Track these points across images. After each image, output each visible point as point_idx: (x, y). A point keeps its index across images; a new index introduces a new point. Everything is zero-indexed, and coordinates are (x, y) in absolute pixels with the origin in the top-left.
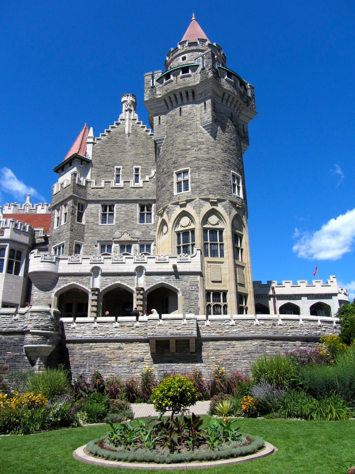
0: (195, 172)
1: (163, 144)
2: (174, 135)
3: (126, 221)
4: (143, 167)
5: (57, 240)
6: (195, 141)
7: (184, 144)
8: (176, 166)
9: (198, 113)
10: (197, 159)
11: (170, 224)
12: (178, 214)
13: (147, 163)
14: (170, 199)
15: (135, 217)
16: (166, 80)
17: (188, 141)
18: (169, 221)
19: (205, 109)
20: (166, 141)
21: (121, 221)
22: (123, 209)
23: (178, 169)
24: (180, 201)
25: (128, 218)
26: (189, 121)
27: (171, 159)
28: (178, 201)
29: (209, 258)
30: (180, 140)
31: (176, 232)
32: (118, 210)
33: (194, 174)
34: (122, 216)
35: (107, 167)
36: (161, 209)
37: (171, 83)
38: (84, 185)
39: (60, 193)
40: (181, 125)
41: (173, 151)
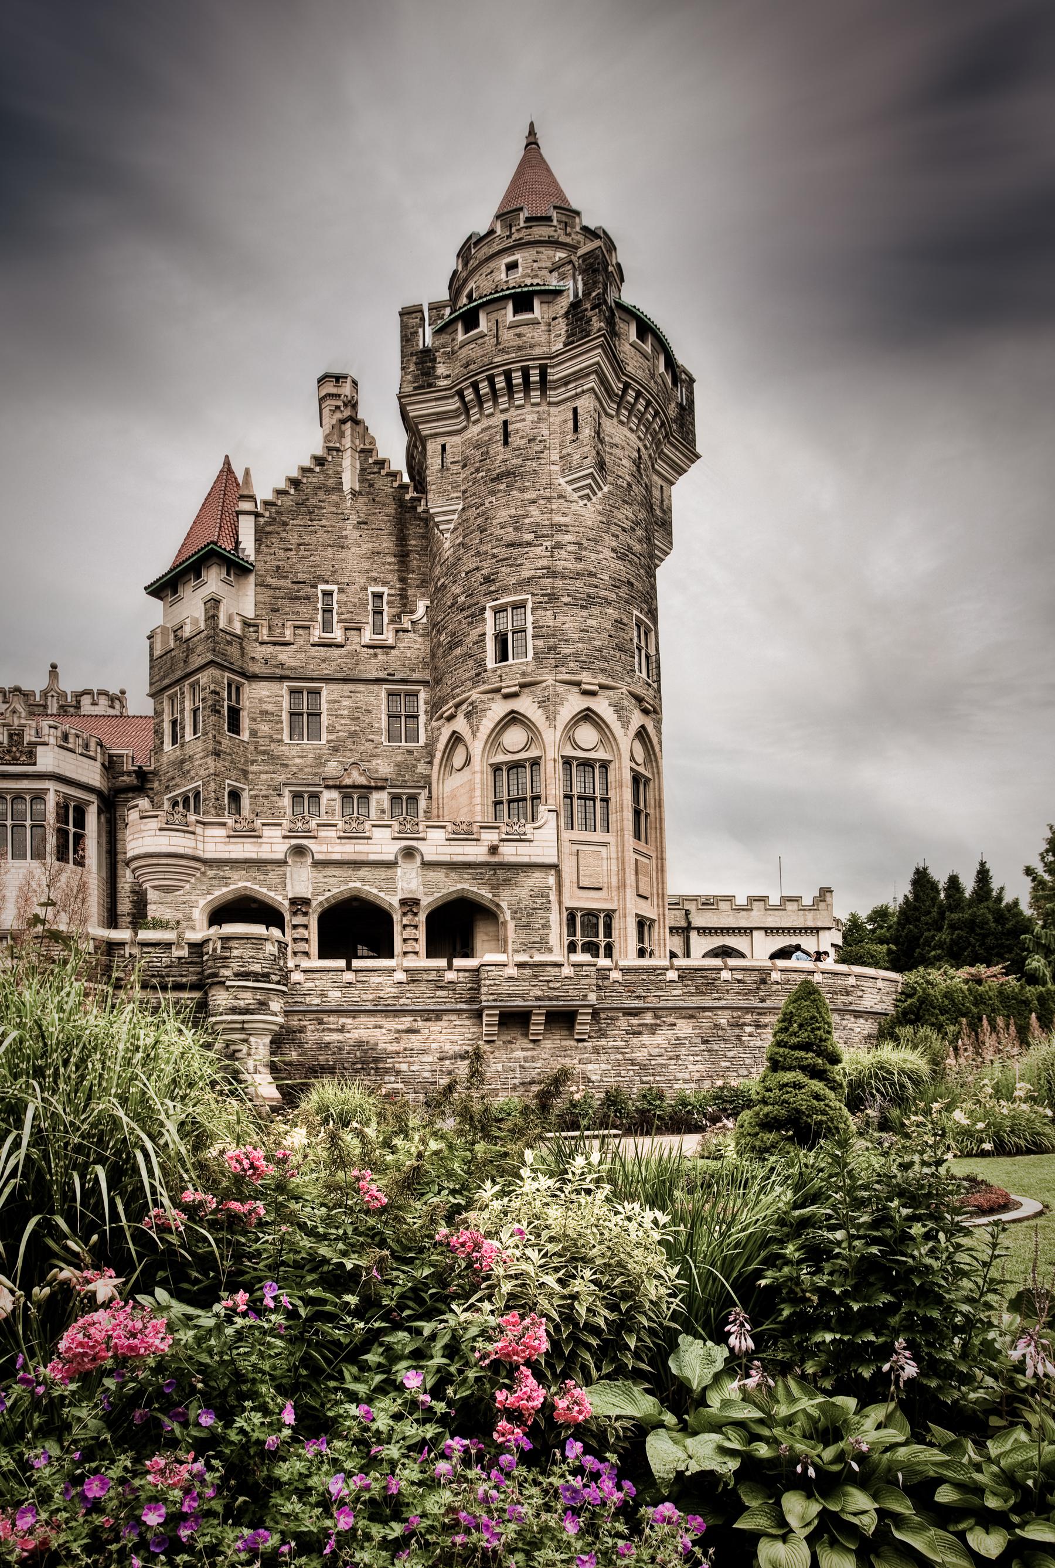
0: (545, 609)
2: (487, 502)
3: (354, 735)
5: (177, 780)
6: (548, 523)
7: (516, 529)
8: (493, 588)
9: (555, 441)
10: (552, 573)
11: (477, 747)
12: (498, 719)
14: (477, 678)
15: (377, 725)
16: (467, 331)
17: (527, 521)
18: (474, 734)
19: (576, 429)
20: (464, 518)
21: (341, 734)
22: (345, 703)
23: (497, 599)
24: (503, 685)
25: (357, 728)
26: (529, 463)
27: (477, 569)
28: (497, 685)
29: (577, 834)
30: (503, 515)
31: (491, 765)
32: (331, 706)
33: (543, 613)
34: (343, 722)
36: (450, 704)
37: (480, 341)
38: (238, 632)
40: (508, 474)
41: (483, 548)
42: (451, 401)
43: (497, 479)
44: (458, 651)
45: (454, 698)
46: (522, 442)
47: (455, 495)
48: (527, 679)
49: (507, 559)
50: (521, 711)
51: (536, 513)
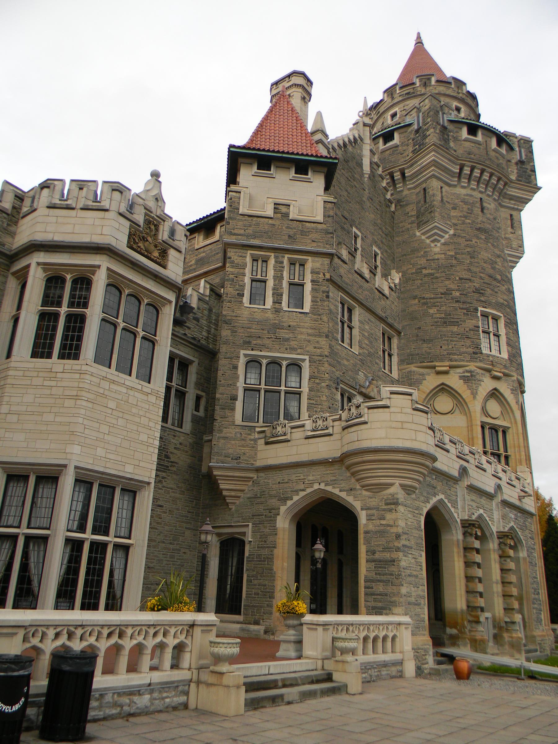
1: (443, 241)
4: (383, 257)
8: (482, 299)
13: (386, 251)
22: (367, 327)
23: (485, 308)
30: (484, 255)
35: (344, 220)
36: (447, 363)
39: (270, 221)
41: (472, 268)
43: (479, 229)
44: (455, 329)
45: (451, 360)
46: (491, 217)
47: (449, 223)
49: (489, 284)
50: (502, 391)
51: (500, 264)
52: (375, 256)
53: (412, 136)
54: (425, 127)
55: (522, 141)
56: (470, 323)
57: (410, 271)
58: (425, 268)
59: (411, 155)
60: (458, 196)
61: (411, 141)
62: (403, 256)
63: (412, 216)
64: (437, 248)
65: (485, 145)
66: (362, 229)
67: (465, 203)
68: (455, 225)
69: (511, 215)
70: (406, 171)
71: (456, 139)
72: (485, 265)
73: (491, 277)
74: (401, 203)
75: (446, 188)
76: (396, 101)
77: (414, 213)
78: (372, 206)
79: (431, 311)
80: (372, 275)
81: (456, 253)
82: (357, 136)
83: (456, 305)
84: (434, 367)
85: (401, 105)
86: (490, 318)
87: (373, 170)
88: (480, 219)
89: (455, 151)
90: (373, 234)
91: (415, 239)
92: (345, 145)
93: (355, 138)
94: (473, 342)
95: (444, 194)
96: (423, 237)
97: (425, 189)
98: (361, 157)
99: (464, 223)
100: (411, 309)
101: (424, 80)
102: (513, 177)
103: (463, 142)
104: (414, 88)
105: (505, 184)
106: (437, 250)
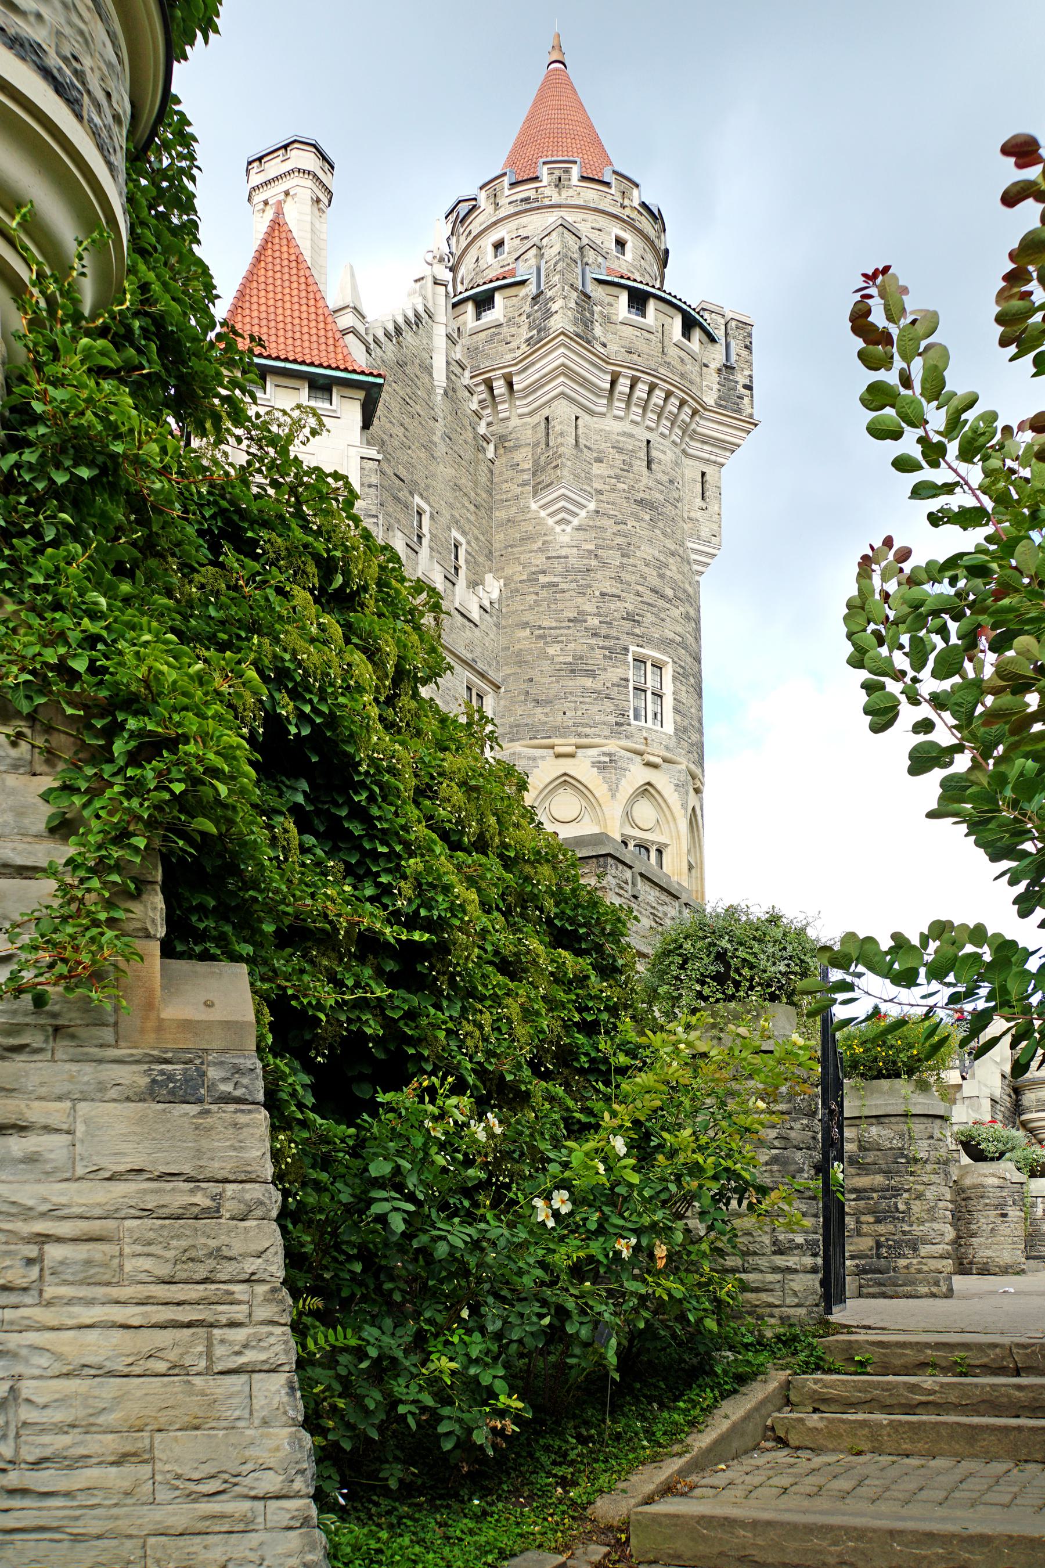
1: (576, 522)
8: (637, 631)
13: (477, 539)
35: (397, 481)
41: (626, 577)
42: (601, 375)
43: (640, 502)
44: (588, 682)
46: (665, 478)
47: (589, 489)
48: (669, 755)
51: (674, 568)
52: (456, 547)
53: (527, 308)
54: (549, 294)
55: (733, 323)
56: (613, 674)
57: (517, 578)
58: (544, 572)
59: (524, 347)
60: (606, 435)
61: (524, 317)
62: (506, 547)
63: (524, 471)
64: (564, 536)
65: (660, 335)
66: (431, 498)
67: (620, 450)
68: (600, 492)
69: (703, 474)
70: (515, 379)
71: (608, 320)
72: (646, 570)
73: (655, 591)
74: (506, 444)
75: (585, 418)
76: (502, 213)
77: (527, 465)
78: (450, 451)
79: (551, 651)
80: (449, 585)
81: (598, 547)
82: (420, 309)
83: (592, 641)
84: (552, 747)
85: (513, 224)
86: (649, 664)
87: (453, 377)
88: (645, 481)
89: (604, 345)
90: (451, 506)
91: (529, 516)
92: (398, 330)
93: (417, 315)
94: (617, 705)
95: (580, 431)
96: (543, 514)
97: (547, 419)
98: (429, 351)
99: (613, 490)
100: (517, 647)
101: (557, 173)
102: (710, 399)
103: (619, 327)
104: (537, 188)
105: (695, 412)
106: (565, 539)
